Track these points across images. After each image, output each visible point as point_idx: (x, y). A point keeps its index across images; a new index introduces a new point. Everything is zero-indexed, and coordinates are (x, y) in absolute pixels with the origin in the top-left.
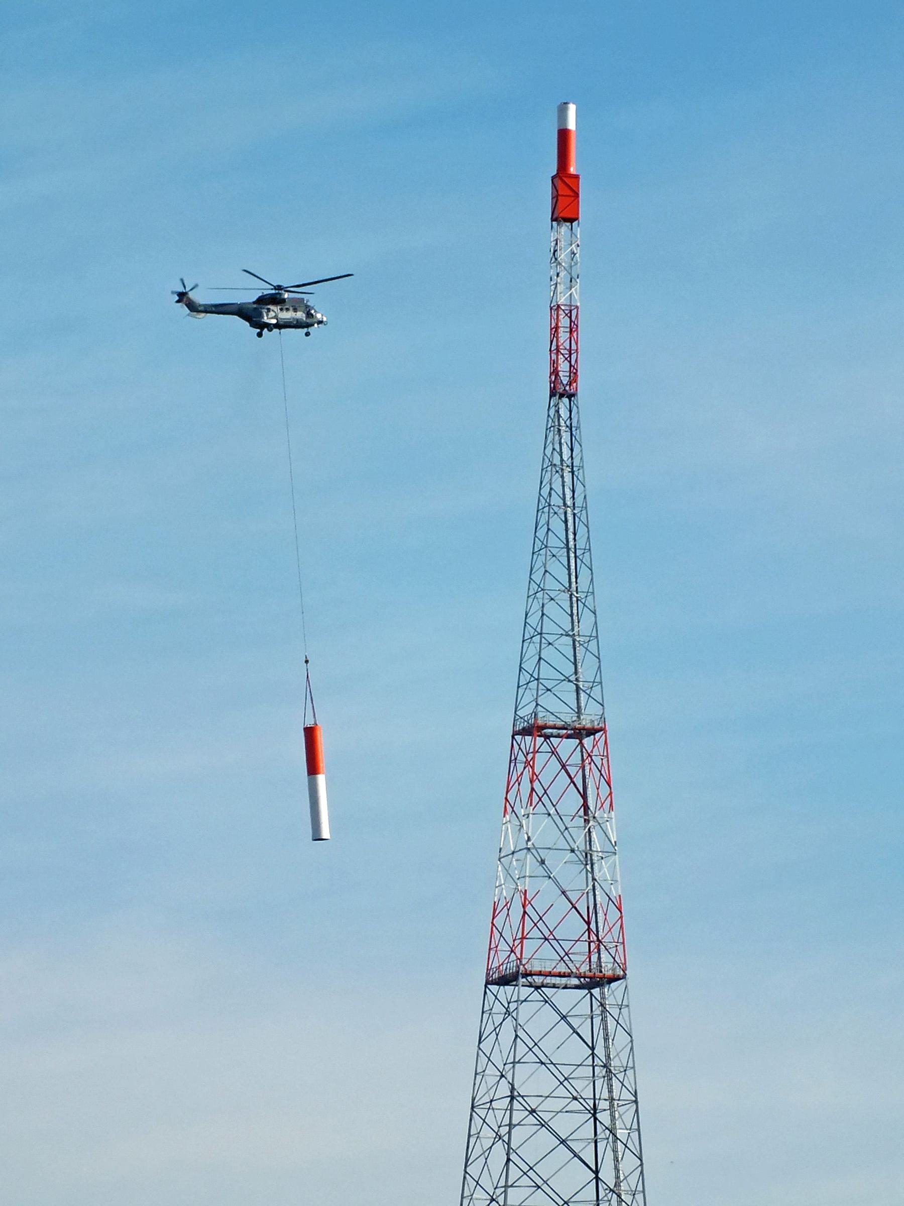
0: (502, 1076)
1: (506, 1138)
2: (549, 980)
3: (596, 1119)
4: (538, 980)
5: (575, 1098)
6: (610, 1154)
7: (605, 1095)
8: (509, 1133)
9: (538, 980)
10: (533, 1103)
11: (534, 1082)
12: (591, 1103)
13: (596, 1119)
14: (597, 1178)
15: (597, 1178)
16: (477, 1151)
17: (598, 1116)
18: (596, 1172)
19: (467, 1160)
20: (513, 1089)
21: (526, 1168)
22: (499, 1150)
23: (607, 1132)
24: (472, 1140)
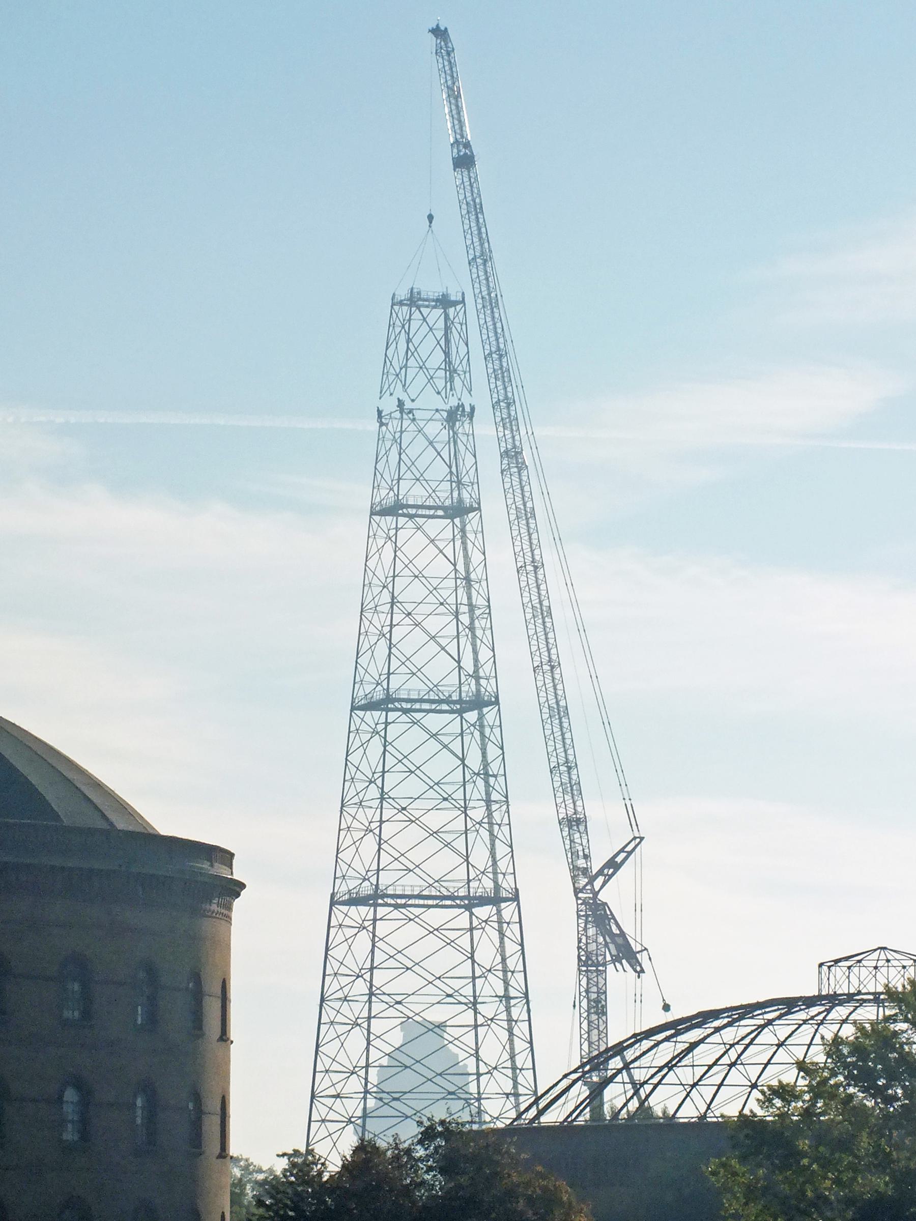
0: (384, 587)
1: (388, 636)
2: (420, 512)
3: (458, 620)
4: (412, 511)
5: (442, 604)
6: (469, 648)
7: (465, 601)
8: (391, 631)
9: (412, 511)
10: (409, 607)
11: (411, 592)
12: (454, 607)
13: (458, 620)
14: (460, 668)
15: (460, 668)
16: (366, 646)
17: (460, 617)
18: (459, 662)
19: (358, 654)
20: (393, 597)
21: (404, 659)
22: (383, 644)
23: (467, 630)
24: (362, 637)
